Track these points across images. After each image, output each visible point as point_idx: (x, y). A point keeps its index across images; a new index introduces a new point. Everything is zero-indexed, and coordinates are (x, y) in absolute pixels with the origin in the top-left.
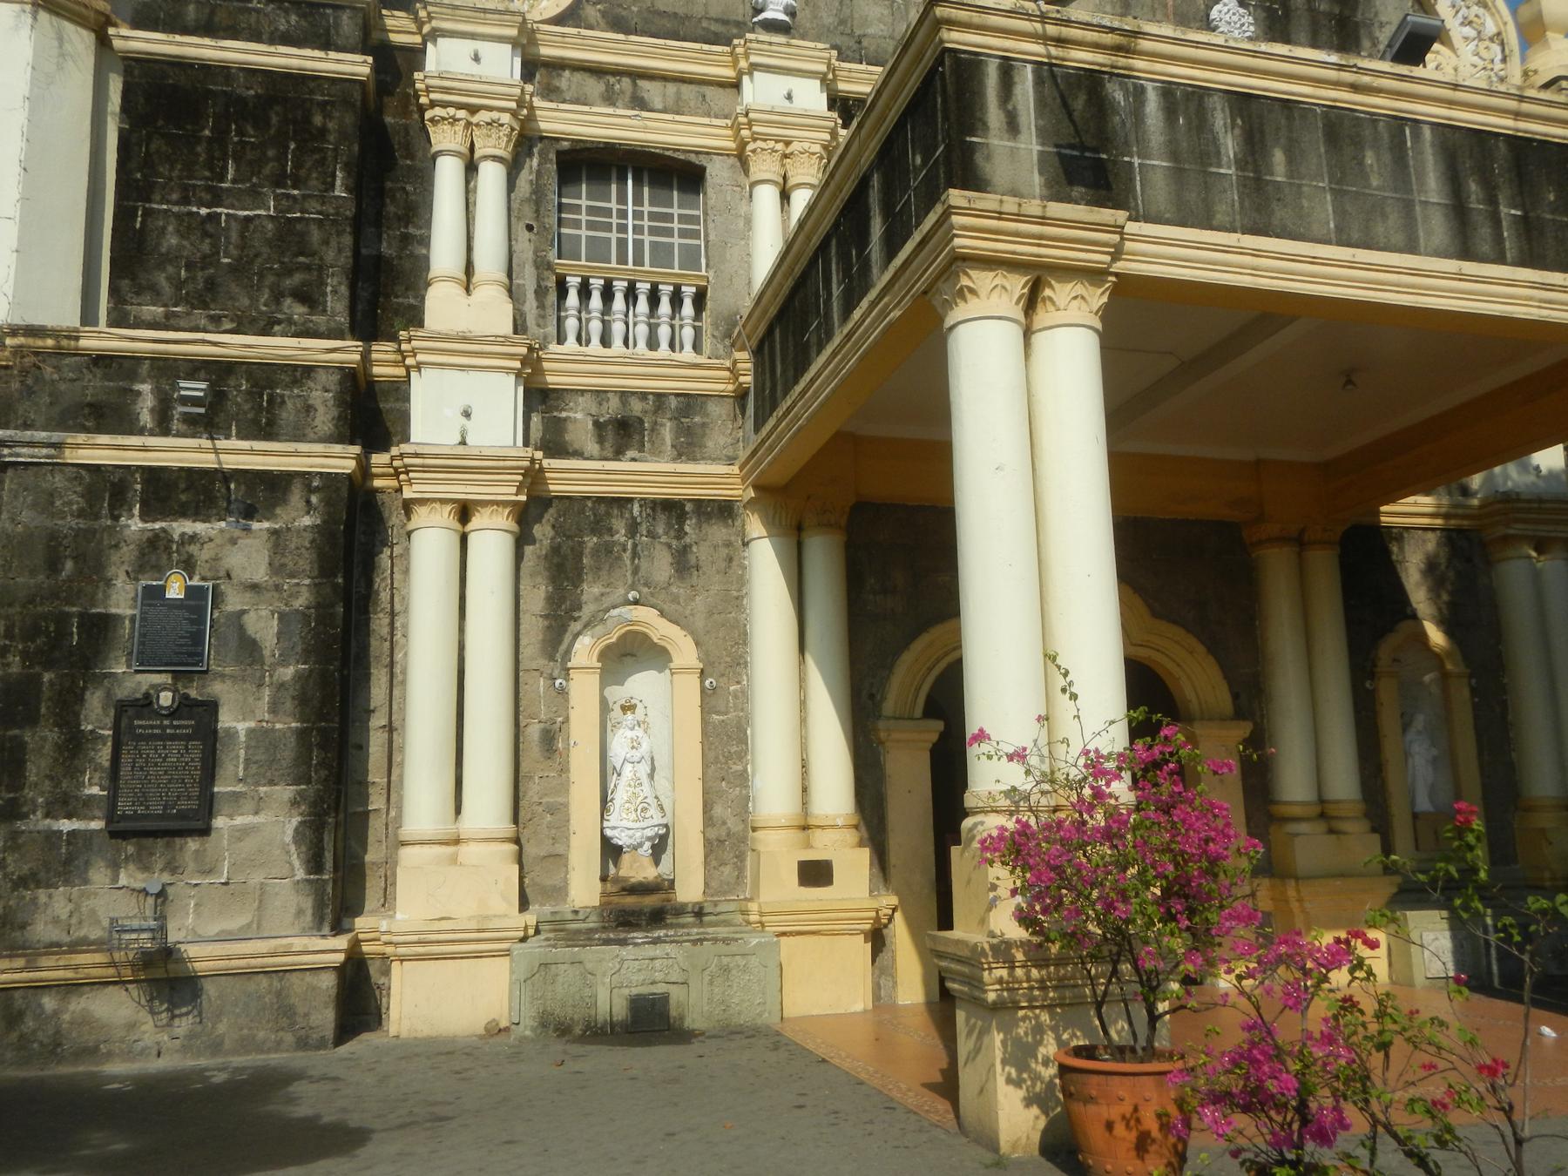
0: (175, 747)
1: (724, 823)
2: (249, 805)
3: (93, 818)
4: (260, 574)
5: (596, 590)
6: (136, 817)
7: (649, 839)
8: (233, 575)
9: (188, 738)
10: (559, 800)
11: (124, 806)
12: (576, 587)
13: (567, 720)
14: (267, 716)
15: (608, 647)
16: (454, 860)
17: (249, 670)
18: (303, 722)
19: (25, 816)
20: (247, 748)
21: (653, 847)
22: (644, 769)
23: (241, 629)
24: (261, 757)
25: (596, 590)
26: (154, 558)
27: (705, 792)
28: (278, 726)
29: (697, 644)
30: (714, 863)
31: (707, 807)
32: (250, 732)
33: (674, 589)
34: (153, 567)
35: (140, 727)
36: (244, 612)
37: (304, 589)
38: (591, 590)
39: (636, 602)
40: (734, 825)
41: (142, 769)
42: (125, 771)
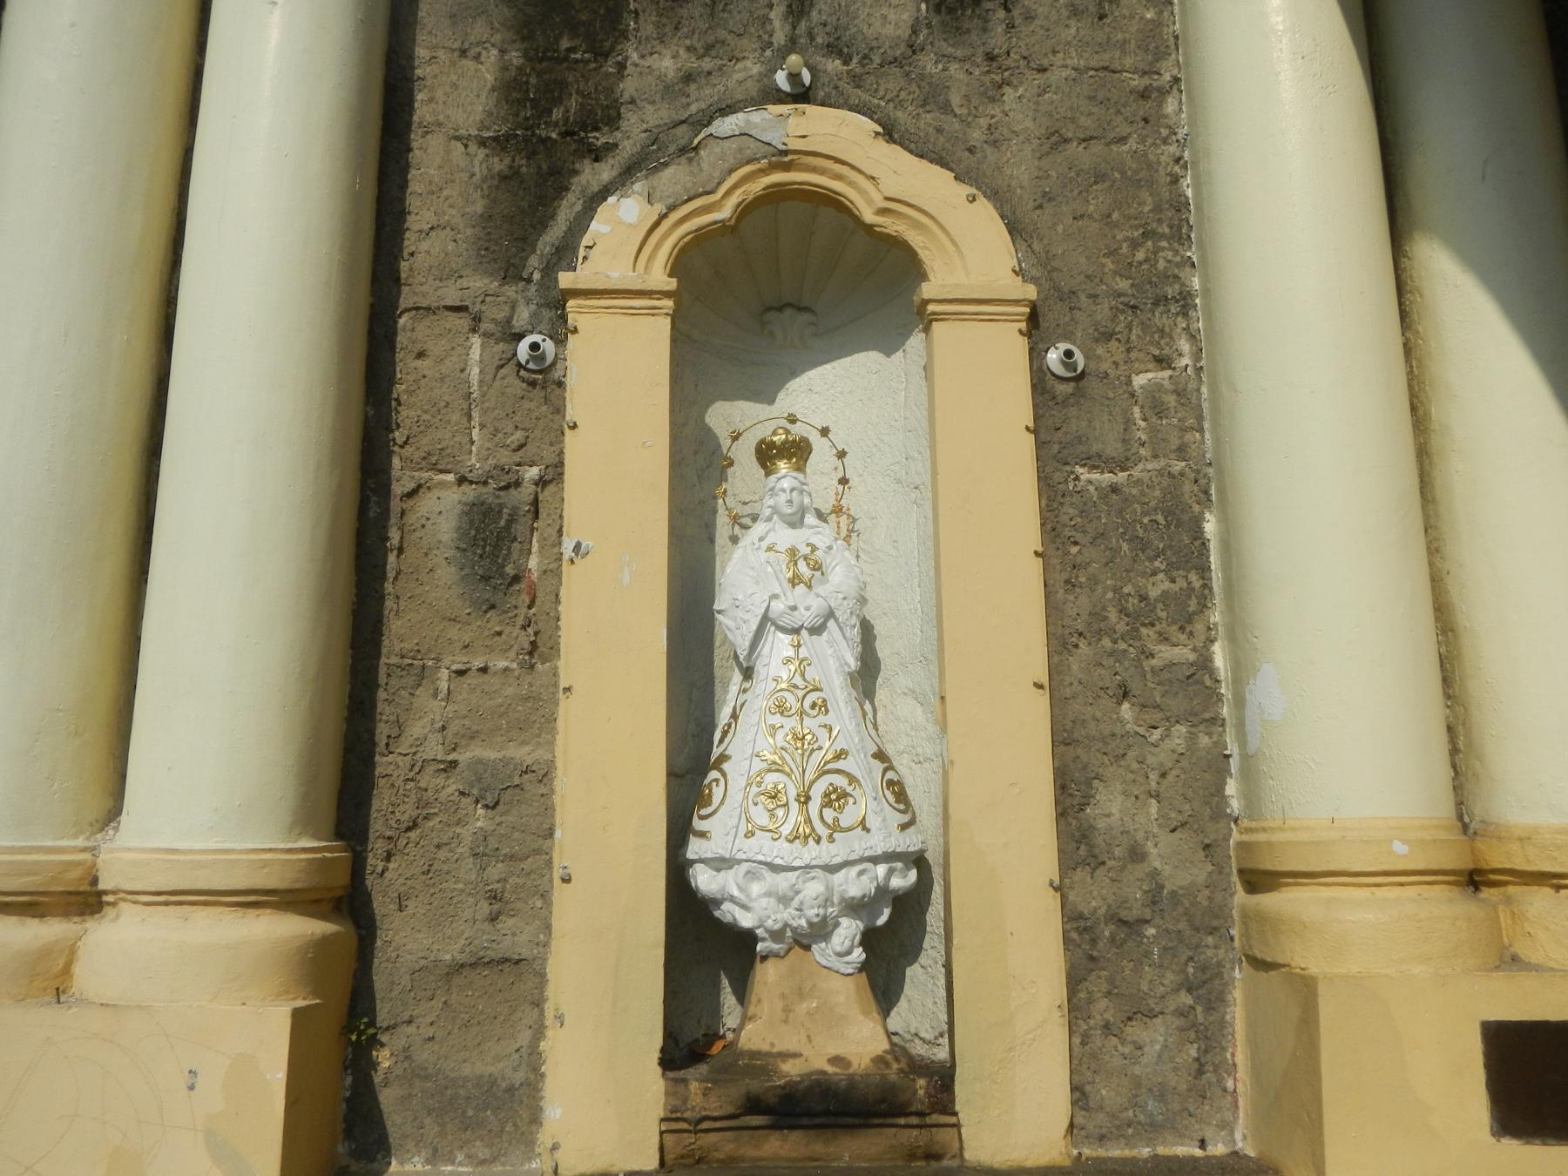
1: (1136, 854)
5: (667, 64)
7: (854, 907)
10: (522, 753)
12: (602, 54)
13: (553, 475)
15: (701, 238)
16: (53, 981)
21: (869, 939)
22: (834, 656)
25: (667, 64)
27: (1063, 738)
29: (1013, 229)
30: (1103, 1010)
31: (1071, 794)
33: (928, 63)
38: (651, 65)
39: (802, 95)
40: (1172, 860)
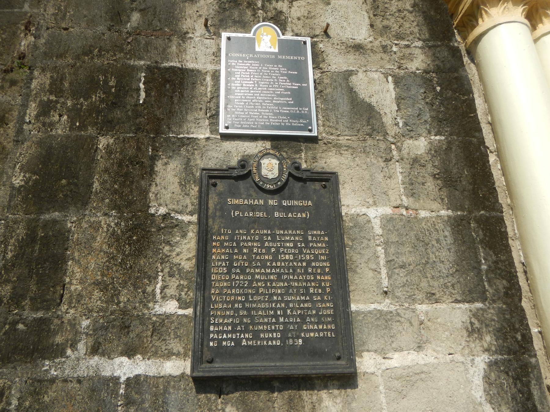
0: (290, 238)
2: (406, 336)
3: (169, 355)
4: (362, 34)
6: (237, 352)
8: (331, 32)
9: (306, 225)
11: (221, 334)
14: (406, 201)
17: (370, 142)
18: (451, 206)
19: (58, 352)
20: (387, 244)
23: (351, 92)
24: (408, 257)
26: (236, 14)
28: (423, 214)
32: (387, 221)
34: (235, 22)
35: (237, 207)
36: (349, 74)
37: (418, 51)
41: (243, 270)
42: (217, 272)
